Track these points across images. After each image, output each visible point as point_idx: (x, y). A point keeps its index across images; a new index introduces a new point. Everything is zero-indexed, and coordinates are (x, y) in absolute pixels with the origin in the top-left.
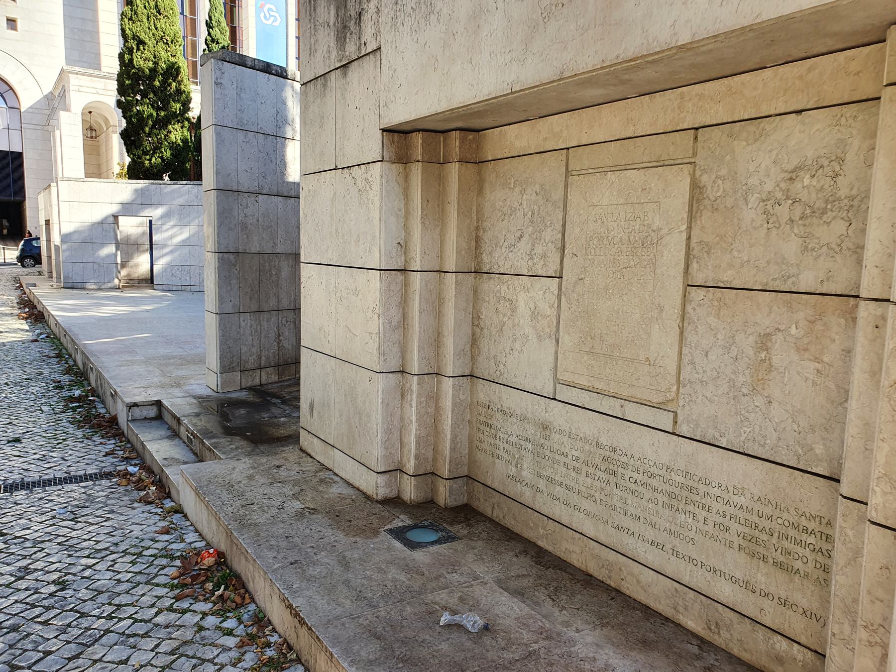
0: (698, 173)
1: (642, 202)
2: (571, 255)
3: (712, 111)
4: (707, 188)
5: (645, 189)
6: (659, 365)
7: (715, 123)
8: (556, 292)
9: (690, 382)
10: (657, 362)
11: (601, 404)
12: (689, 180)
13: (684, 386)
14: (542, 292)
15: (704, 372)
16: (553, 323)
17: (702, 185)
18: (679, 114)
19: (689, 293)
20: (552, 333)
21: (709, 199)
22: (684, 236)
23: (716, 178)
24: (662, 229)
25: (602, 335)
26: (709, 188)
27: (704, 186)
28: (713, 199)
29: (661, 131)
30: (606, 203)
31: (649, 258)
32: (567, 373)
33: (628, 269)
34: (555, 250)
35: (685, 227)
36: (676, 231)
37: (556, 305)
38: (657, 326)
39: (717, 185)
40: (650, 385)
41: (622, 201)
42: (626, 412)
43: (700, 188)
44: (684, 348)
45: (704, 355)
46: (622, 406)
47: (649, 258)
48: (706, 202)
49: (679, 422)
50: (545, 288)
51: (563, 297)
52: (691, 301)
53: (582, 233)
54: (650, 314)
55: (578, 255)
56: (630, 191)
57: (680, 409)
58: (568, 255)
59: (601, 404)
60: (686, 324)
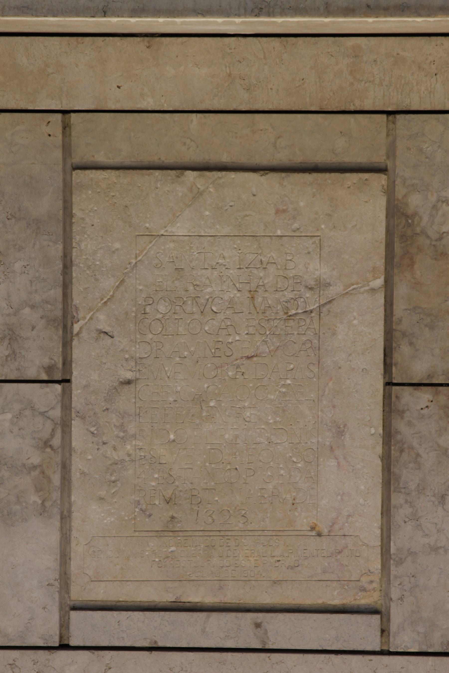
0: (400, 191)
1: (279, 233)
2: (94, 335)
3: (423, 89)
4: (421, 218)
5: (284, 211)
6: (341, 533)
7: (429, 108)
8: (57, 413)
9: (412, 554)
10: (337, 527)
11: (203, 631)
12: (382, 202)
13: (400, 562)
14: (9, 416)
15: (438, 531)
16: (49, 480)
17: (410, 211)
18: (352, 84)
19: (397, 397)
20: (48, 504)
21: (428, 237)
22: (381, 300)
23: (438, 201)
24: (329, 285)
25: (195, 493)
26: (425, 219)
27: (415, 214)
28: (434, 236)
29: (313, 109)
30: (185, 232)
31: (304, 338)
32: (103, 584)
33: (255, 359)
34: (43, 321)
35: (380, 282)
36: (362, 290)
37: (57, 441)
38: (333, 463)
39: (440, 213)
40: (324, 572)
41: (226, 230)
42: (270, 634)
43: (407, 216)
44: (394, 496)
45: (436, 503)
46: (258, 625)
47: (304, 338)
48: (421, 240)
49: (393, 627)
50: (17, 407)
51: (76, 425)
52: (403, 412)
53: (122, 288)
54: (314, 440)
55: (115, 334)
56: (248, 213)
57: (393, 605)
58: (84, 334)
59: (203, 631)
60: (394, 453)
